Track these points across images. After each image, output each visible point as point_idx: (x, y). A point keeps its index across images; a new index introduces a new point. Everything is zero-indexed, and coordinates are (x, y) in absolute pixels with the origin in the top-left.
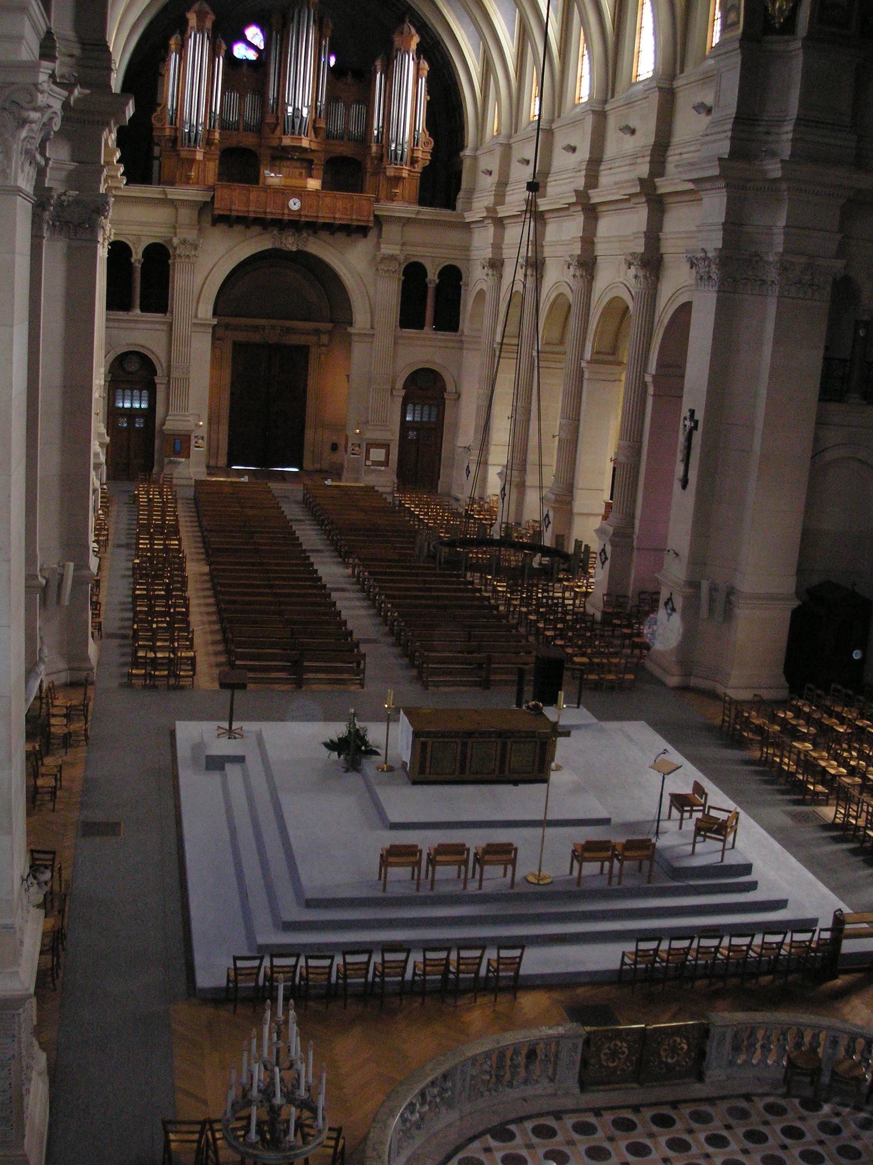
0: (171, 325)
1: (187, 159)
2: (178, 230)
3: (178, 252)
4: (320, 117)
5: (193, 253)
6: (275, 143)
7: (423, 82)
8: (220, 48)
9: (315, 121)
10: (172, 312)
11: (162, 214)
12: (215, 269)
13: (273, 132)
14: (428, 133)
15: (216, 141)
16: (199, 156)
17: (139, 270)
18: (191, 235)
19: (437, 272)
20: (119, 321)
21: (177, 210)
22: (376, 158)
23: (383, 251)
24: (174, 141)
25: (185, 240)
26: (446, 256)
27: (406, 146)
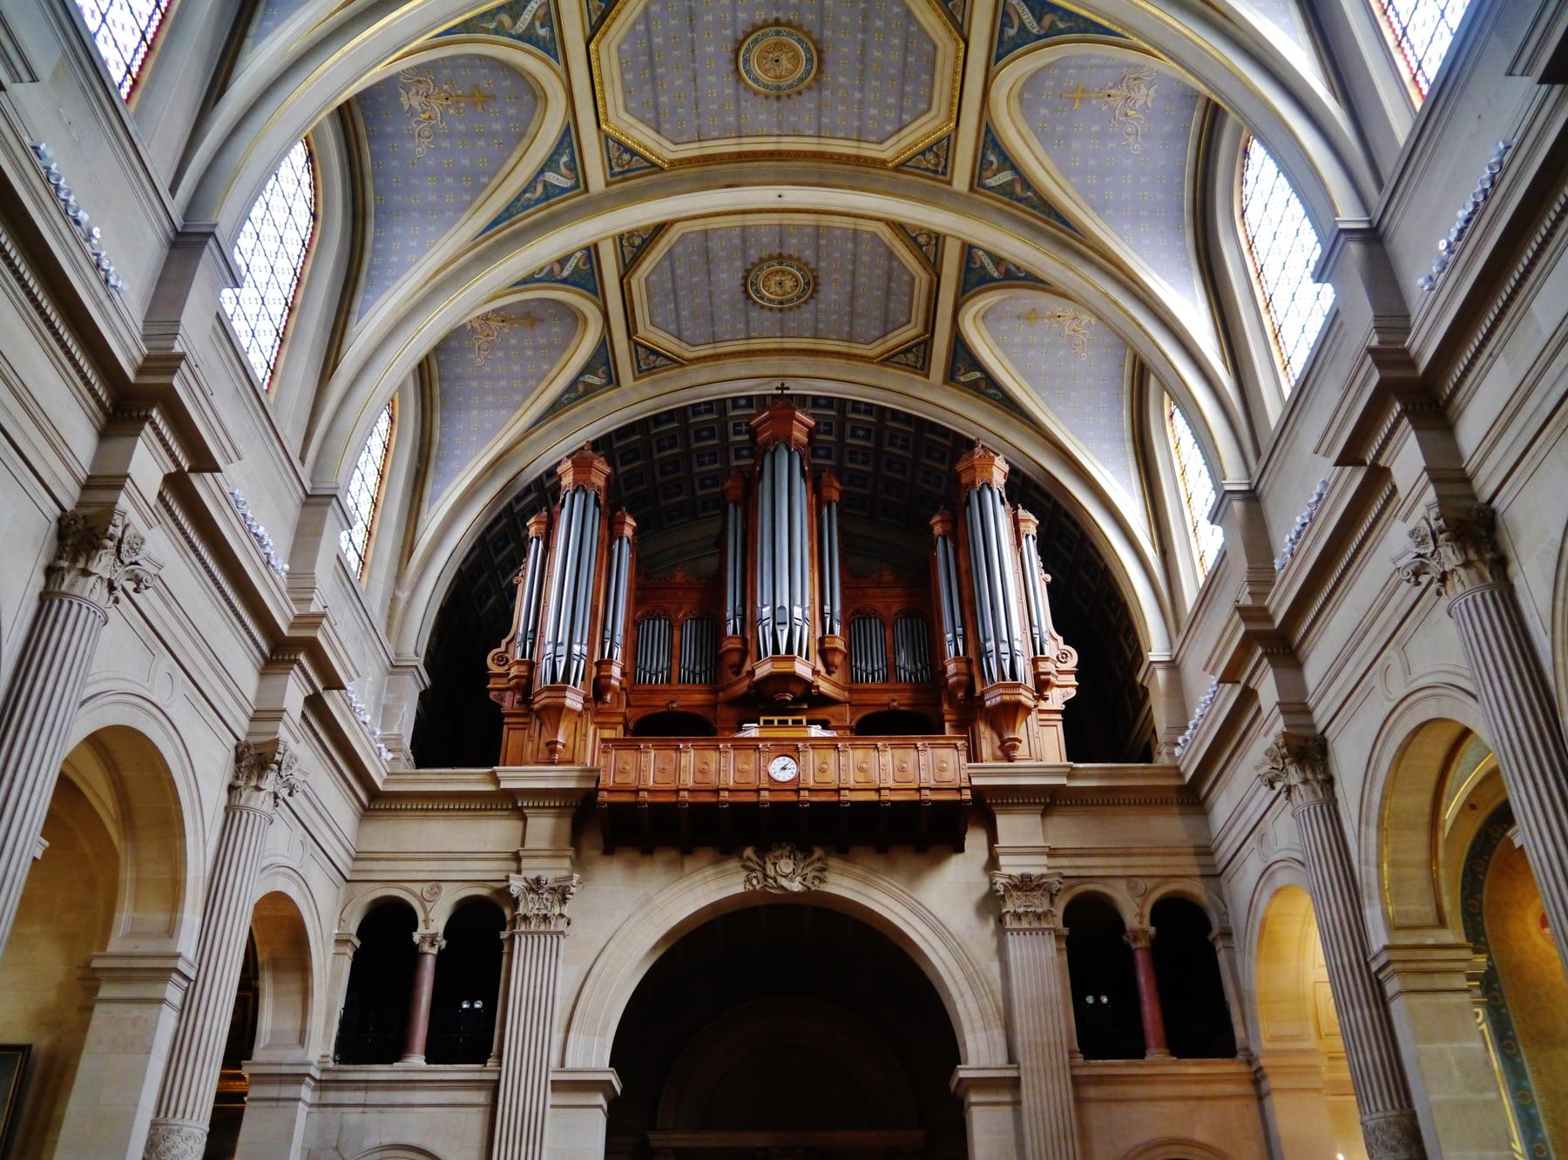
0: (494, 1088)
1: (545, 707)
2: (525, 863)
3: (521, 910)
4: (832, 631)
5: (557, 911)
6: (743, 687)
7: (1030, 546)
8: (623, 523)
9: (822, 641)
10: (500, 1056)
11: (495, 833)
12: (612, 946)
13: (738, 672)
14: (1060, 639)
15: (614, 682)
16: (574, 701)
17: (429, 964)
18: (552, 871)
19: (1148, 910)
20: (368, 1085)
21: (524, 819)
22: (958, 684)
23: (1004, 871)
24: (525, 687)
25: (538, 880)
26: (1156, 871)
27: (1017, 646)
